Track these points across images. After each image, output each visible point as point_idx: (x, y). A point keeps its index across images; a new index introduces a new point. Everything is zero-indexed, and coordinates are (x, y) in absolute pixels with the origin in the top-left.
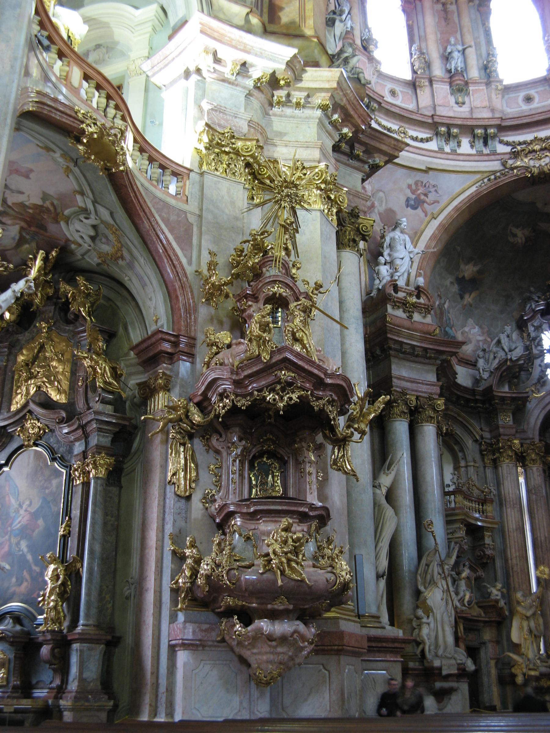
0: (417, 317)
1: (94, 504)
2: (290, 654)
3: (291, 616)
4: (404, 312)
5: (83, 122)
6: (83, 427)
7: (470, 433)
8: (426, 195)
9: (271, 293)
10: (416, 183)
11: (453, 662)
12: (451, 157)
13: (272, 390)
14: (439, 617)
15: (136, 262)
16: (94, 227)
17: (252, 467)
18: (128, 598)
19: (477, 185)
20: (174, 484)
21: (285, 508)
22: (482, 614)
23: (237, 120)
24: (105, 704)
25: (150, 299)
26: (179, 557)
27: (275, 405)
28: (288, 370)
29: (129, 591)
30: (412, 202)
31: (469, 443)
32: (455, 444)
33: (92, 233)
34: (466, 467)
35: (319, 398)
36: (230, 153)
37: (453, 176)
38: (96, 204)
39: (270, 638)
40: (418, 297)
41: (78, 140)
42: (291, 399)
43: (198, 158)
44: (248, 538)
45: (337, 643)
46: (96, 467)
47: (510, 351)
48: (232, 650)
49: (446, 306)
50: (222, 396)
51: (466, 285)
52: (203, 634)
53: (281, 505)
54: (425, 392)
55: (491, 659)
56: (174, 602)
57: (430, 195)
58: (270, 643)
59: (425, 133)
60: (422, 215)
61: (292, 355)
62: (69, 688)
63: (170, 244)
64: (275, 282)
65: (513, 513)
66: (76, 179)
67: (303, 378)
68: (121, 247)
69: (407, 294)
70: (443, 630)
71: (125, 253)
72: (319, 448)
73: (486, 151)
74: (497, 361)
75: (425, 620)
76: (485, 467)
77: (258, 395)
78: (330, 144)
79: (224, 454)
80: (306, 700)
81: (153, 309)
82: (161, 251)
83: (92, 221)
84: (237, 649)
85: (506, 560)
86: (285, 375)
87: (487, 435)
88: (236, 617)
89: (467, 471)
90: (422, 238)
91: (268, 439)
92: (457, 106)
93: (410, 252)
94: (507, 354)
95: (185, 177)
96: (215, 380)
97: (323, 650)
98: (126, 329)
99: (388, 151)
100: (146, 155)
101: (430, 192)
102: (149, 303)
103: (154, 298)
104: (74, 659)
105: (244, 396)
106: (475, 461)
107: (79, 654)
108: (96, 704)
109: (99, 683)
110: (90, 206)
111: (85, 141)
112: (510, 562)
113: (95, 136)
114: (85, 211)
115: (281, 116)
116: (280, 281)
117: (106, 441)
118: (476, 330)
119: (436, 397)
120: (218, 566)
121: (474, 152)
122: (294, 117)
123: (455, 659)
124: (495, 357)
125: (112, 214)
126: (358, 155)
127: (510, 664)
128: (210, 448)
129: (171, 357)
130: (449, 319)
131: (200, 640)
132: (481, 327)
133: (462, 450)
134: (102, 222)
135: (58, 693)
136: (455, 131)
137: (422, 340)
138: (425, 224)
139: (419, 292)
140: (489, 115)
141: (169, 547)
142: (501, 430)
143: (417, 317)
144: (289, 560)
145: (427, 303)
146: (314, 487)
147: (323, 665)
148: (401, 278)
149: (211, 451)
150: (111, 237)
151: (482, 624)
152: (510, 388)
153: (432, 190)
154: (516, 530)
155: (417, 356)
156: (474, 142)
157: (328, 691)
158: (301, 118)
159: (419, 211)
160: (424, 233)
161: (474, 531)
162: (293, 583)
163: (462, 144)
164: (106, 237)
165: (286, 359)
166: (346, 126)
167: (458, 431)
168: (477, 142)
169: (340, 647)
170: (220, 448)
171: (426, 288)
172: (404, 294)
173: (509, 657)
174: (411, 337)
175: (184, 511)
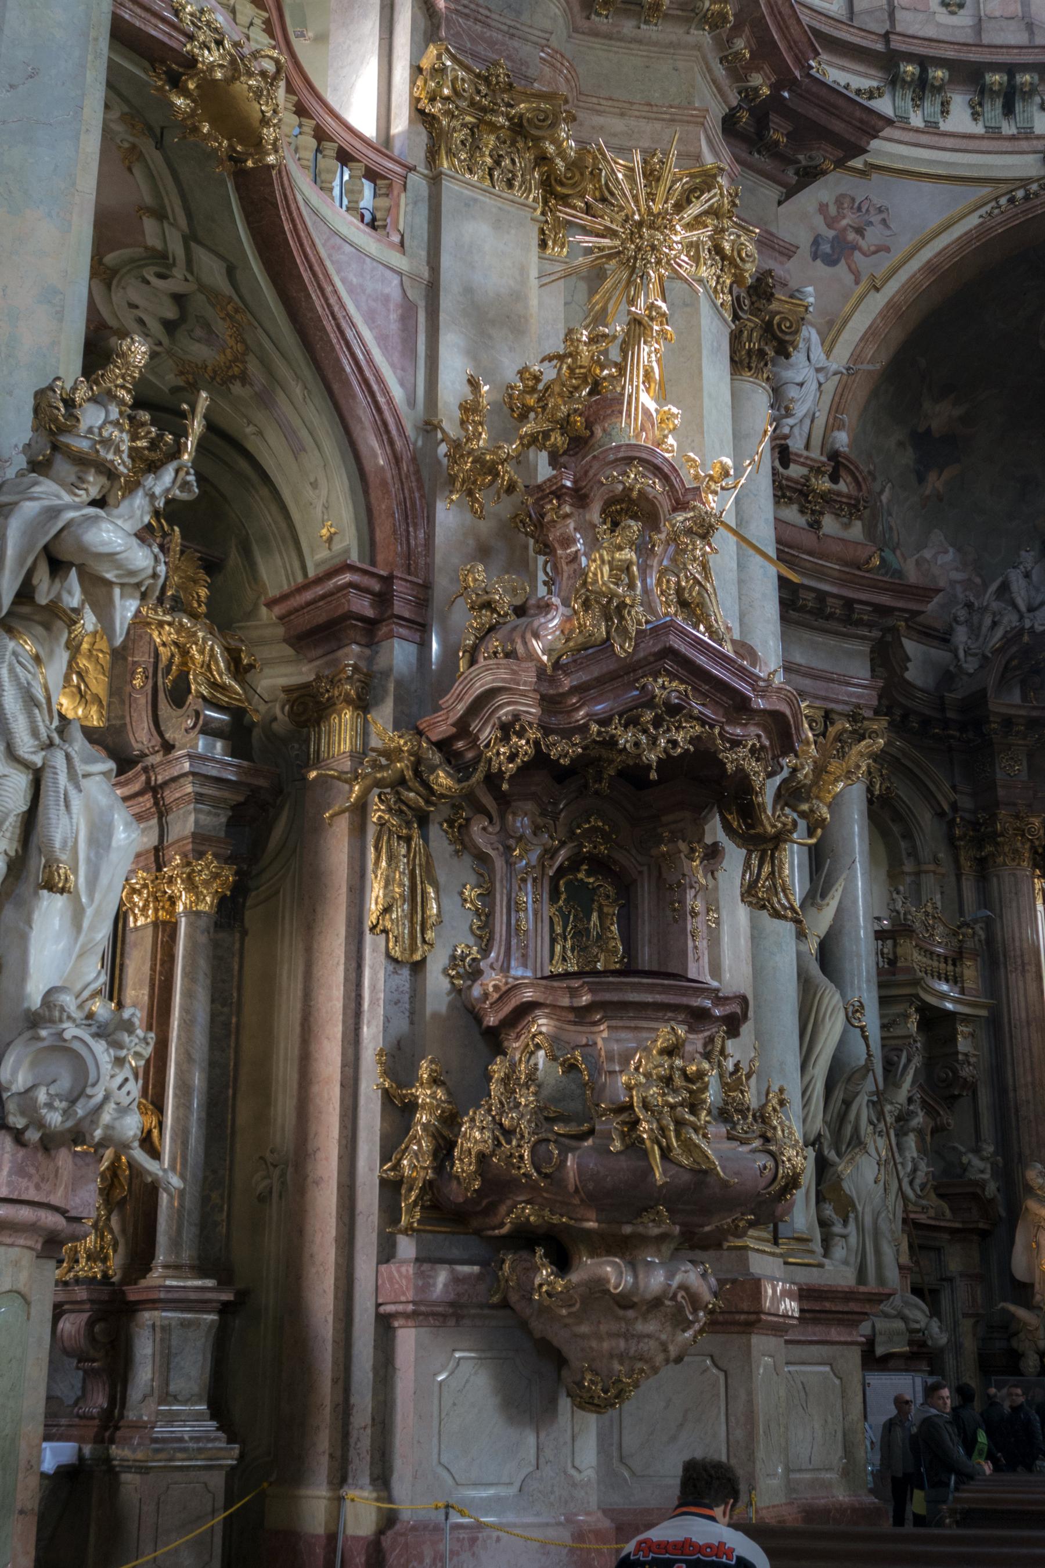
0: (829, 524)
1: (190, 975)
4: (802, 512)
5: (191, 38)
6: (154, 790)
7: (929, 796)
8: (860, 231)
10: (839, 201)
11: (900, 1325)
12: (924, 139)
13: (632, 722)
14: (868, 1220)
15: (281, 393)
16: (179, 299)
18: (263, 1199)
19: (982, 211)
20: (385, 931)
21: (659, 998)
22: (948, 1213)
23: (516, 43)
25: (314, 485)
26: (399, 1110)
27: (639, 756)
28: (673, 676)
29: (266, 1182)
30: (826, 248)
31: (926, 818)
32: (893, 821)
33: (171, 313)
34: (918, 874)
35: (736, 743)
36: (502, 127)
37: (927, 186)
38: (193, 244)
39: (624, 1302)
40: (834, 478)
41: (176, 82)
42: (674, 743)
43: (423, 138)
44: (571, 1068)
45: (745, 1306)
46: (191, 885)
47: (1031, 610)
48: (524, 1325)
49: (884, 498)
50: (506, 730)
51: (931, 450)
54: (846, 703)
55: (965, 1315)
56: (390, 1212)
57: (869, 232)
58: (621, 1313)
59: (866, 76)
60: (849, 278)
62: (131, 1415)
64: (629, 460)
65: (1021, 984)
66: (151, 176)
67: (705, 695)
68: (244, 354)
69: (811, 469)
70: (878, 1252)
71: (253, 368)
72: (714, 853)
73: (1008, 128)
74: (999, 633)
75: (838, 1229)
76: (959, 877)
77: (599, 733)
78: (717, 111)
81: (319, 509)
82: (348, 369)
83: (176, 283)
84: (537, 1326)
85: (1001, 1090)
86: (665, 688)
87: (966, 803)
88: (540, 1251)
89: (919, 885)
90: (845, 335)
91: (595, 829)
92: (944, 10)
93: (818, 370)
94: (1021, 618)
96: (491, 693)
98: (246, 552)
99: (847, 136)
100: (309, 125)
101: (871, 223)
102: (309, 493)
103: (323, 482)
104: (145, 1348)
105: (567, 734)
106: (936, 861)
107: (158, 1336)
110: (176, 248)
111: (191, 86)
112: (1011, 1095)
113: (219, 75)
114: (161, 259)
115: (609, 37)
116: (642, 461)
117: (216, 821)
118: (950, 556)
119: (868, 713)
120: (508, 1133)
121: (979, 129)
122: (640, 42)
123: (904, 1319)
124: (995, 624)
125: (231, 272)
126: (777, 143)
127: (1008, 1327)
129: (371, 630)
130: (891, 529)
132: (959, 550)
133: (908, 835)
134: (202, 288)
135: (104, 1427)
136: (939, 74)
137: (843, 581)
138: (853, 301)
139: (837, 464)
140: (1022, 38)
141: (372, 1083)
142: (1001, 792)
143: (829, 524)
144: (680, 1123)
145: (854, 493)
146: (703, 944)
147: (712, 1357)
148: (796, 430)
149: (467, 859)
150: (222, 327)
151: (946, 1236)
152: (1025, 698)
153: (876, 219)
154: (1028, 1024)
155: (830, 617)
156: (981, 104)
158: (656, 44)
159: (842, 268)
160: (850, 324)
161: (936, 1023)
162: (686, 1177)
163: (953, 107)
164: (207, 326)
166: (758, 69)
167: (903, 791)
168: (987, 107)
169: (753, 1317)
171: (853, 456)
172: (804, 471)
173: (1008, 1312)
174: (819, 573)
175: (406, 997)
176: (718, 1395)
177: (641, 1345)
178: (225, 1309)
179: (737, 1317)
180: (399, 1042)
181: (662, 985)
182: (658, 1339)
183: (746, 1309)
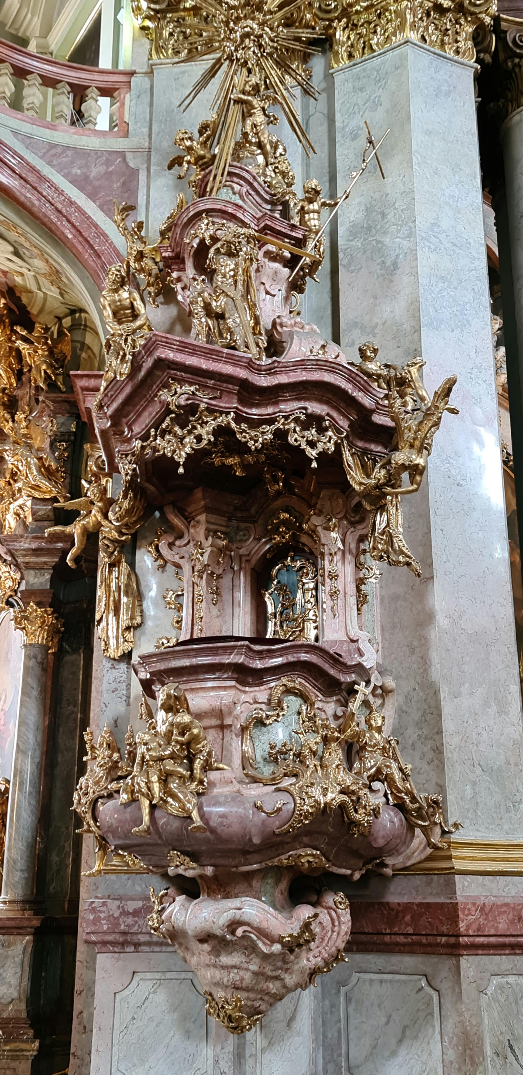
2: (254, 967)
3: (255, 884)
9: (197, 240)
17: (260, 582)
24: (23, 1046)
28: (181, 382)
35: (255, 424)
42: (199, 439)
45: (444, 929)
52: (130, 920)
53: (189, 657)
61: (171, 349)
63: (89, 218)
67: (214, 389)
79: (187, 568)
80: (394, 1054)
82: (70, 236)
86: (178, 395)
95: (123, 92)
97: (421, 944)
108: (8, 1048)
109: (23, 1006)
116: (208, 212)
128: (166, 562)
131: (124, 933)
157: (438, 1037)
165: (161, 363)
169: (452, 940)
170: (177, 559)
176: (432, 1014)
177: (232, 975)
178: (38, 933)
179: (439, 939)
180: (116, 721)
181: (193, 649)
182: (247, 969)
183: (446, 932)
